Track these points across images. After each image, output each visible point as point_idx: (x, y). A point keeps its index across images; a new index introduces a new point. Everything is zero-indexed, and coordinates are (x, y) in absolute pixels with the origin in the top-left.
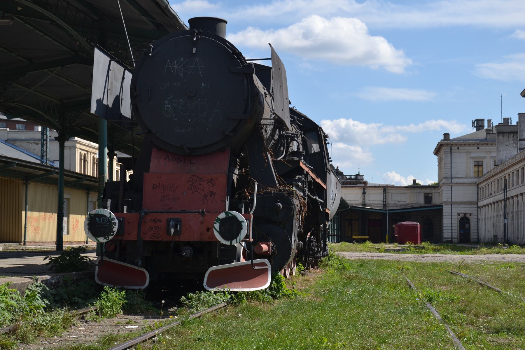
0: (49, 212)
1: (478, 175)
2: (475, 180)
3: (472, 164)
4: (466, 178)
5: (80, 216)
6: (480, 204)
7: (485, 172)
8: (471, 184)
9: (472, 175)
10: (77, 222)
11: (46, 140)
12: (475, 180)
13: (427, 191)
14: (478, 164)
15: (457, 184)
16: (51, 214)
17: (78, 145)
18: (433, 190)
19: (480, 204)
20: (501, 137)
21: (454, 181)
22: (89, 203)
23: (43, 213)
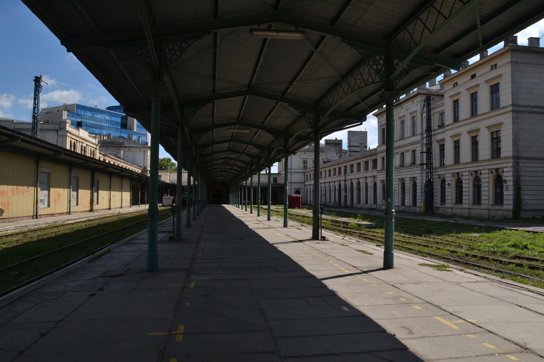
0: (22, 185)
1: (305, 168)
2: (303, 170)
3: (302, 162)
4: (299, 169)
5: (63, 189)
6: (306, 183)
7: (308, 167)
8: (301, 173)
9: (302, 167)
10: (59, 195)
11: (37, 123)
12: (303, 170)
13: (275, 176)
14: (305, 162)
15: (294, 172)
16: (26, 187)
17: (68, 134)
18: (278, 176)
19: (306, 183)
20: (328, 146)
21: (293, 171)
22: (72, 179)
23: (15, 187)
